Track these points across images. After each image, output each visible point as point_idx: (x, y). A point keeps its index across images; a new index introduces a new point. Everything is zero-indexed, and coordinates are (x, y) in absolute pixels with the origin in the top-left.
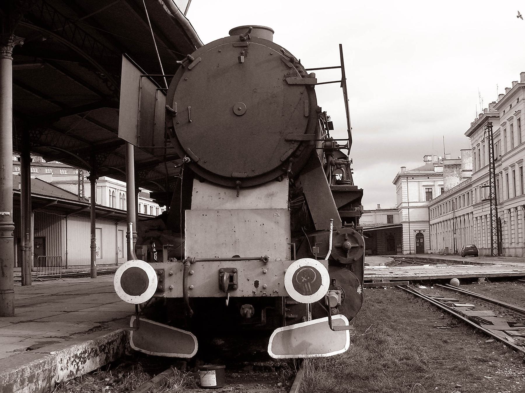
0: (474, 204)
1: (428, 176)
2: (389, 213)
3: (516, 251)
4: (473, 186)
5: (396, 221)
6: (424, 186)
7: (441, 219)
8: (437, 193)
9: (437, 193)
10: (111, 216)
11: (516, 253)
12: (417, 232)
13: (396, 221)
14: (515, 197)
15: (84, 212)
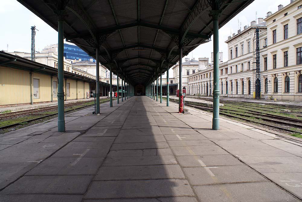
0: (229, 73)
1: (188, 65)
2: (171, 80)
3: (282, 97)
4: (228, 66)
5: (174, 83)
6: (186, 69)
7: (197, 82)
8: (191, 73)
9: (191, 73)
10: (42, 71)
11: (282, 98)
12: (183, 87)
13: (174, 83)
14: (237, 73)
15: (10, 63)
